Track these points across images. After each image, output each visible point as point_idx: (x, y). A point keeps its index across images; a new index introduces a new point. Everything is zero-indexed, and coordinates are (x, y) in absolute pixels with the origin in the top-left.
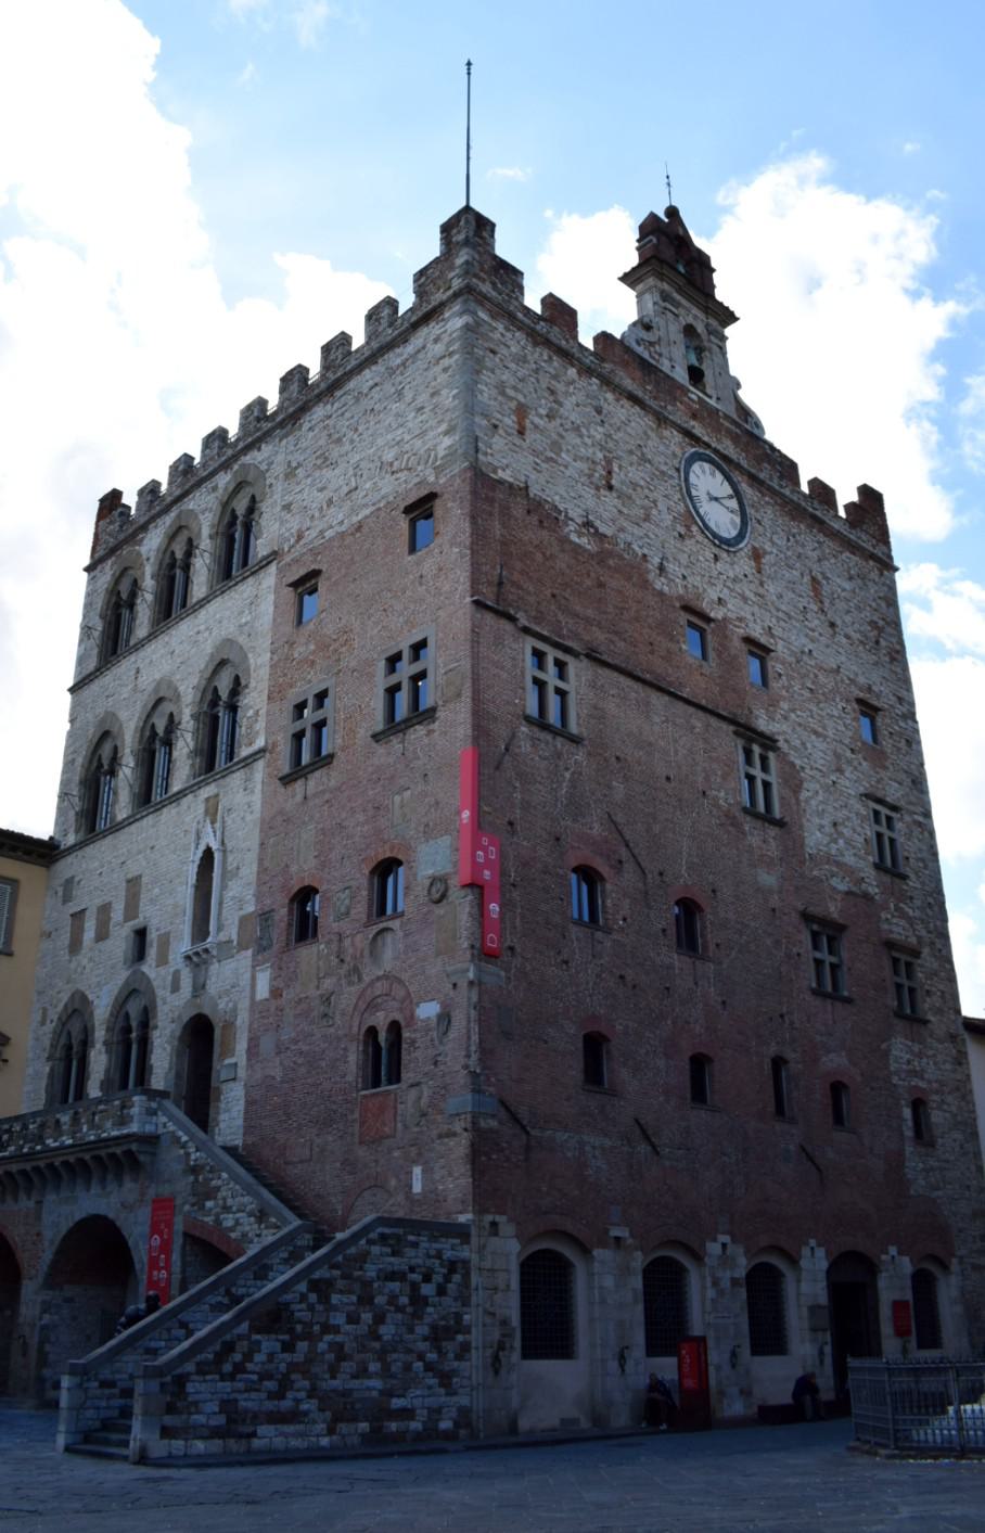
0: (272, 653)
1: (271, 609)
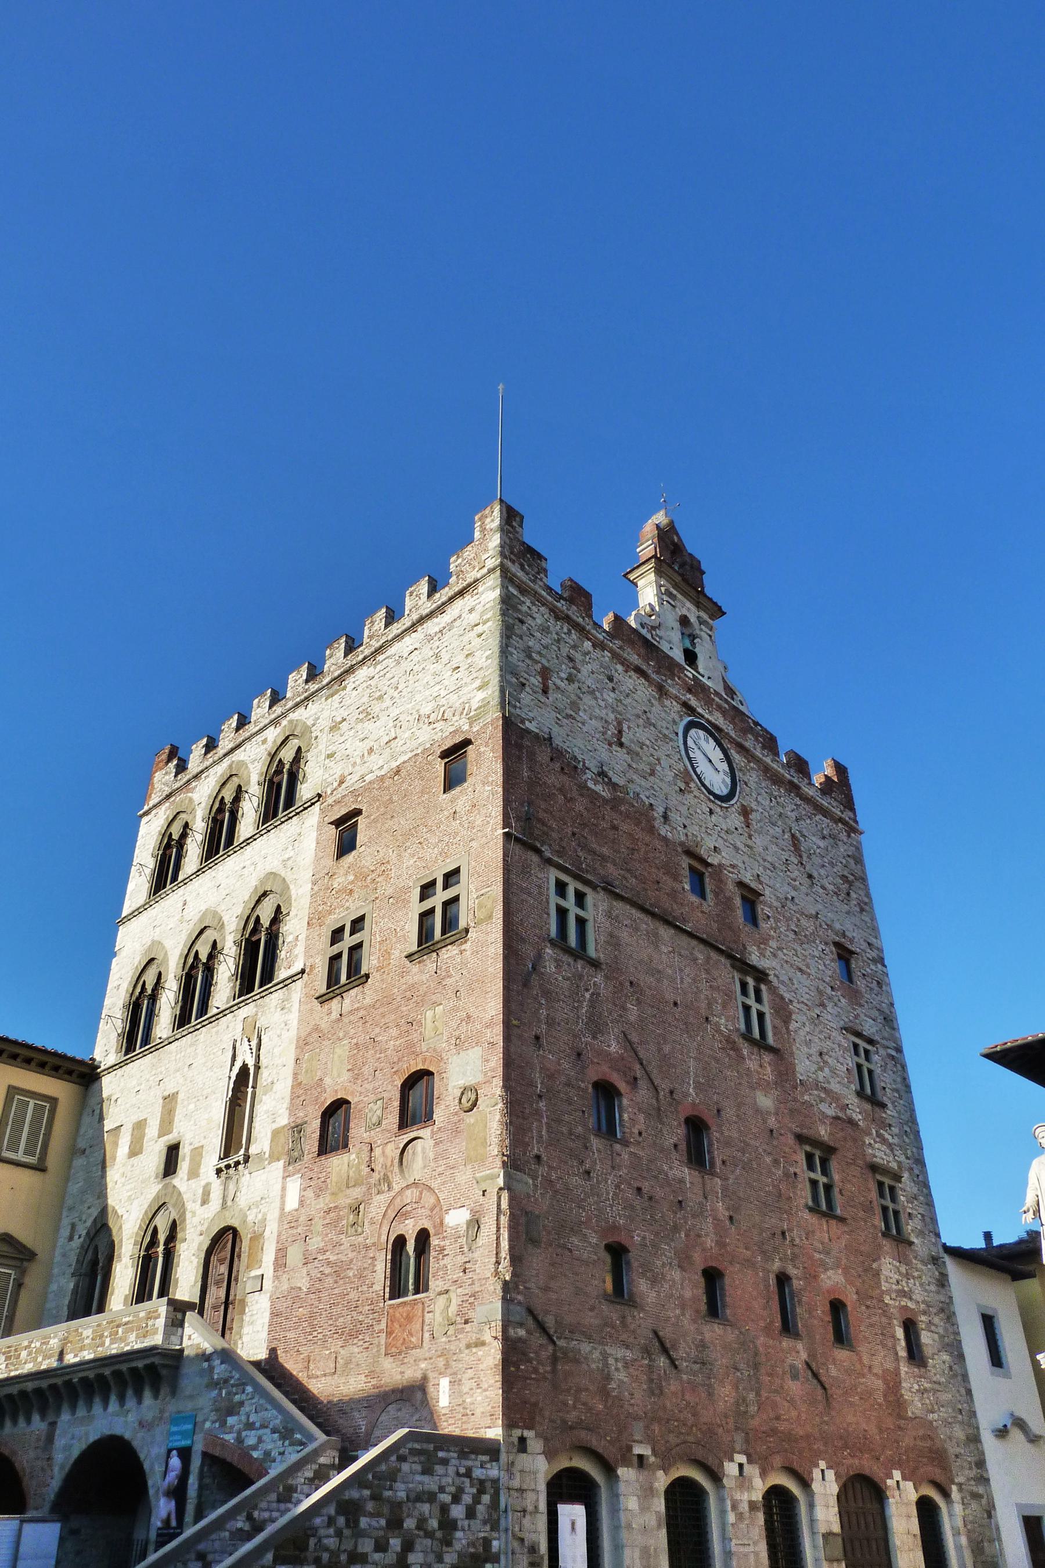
0: (314, 883)
1: (314, 845)
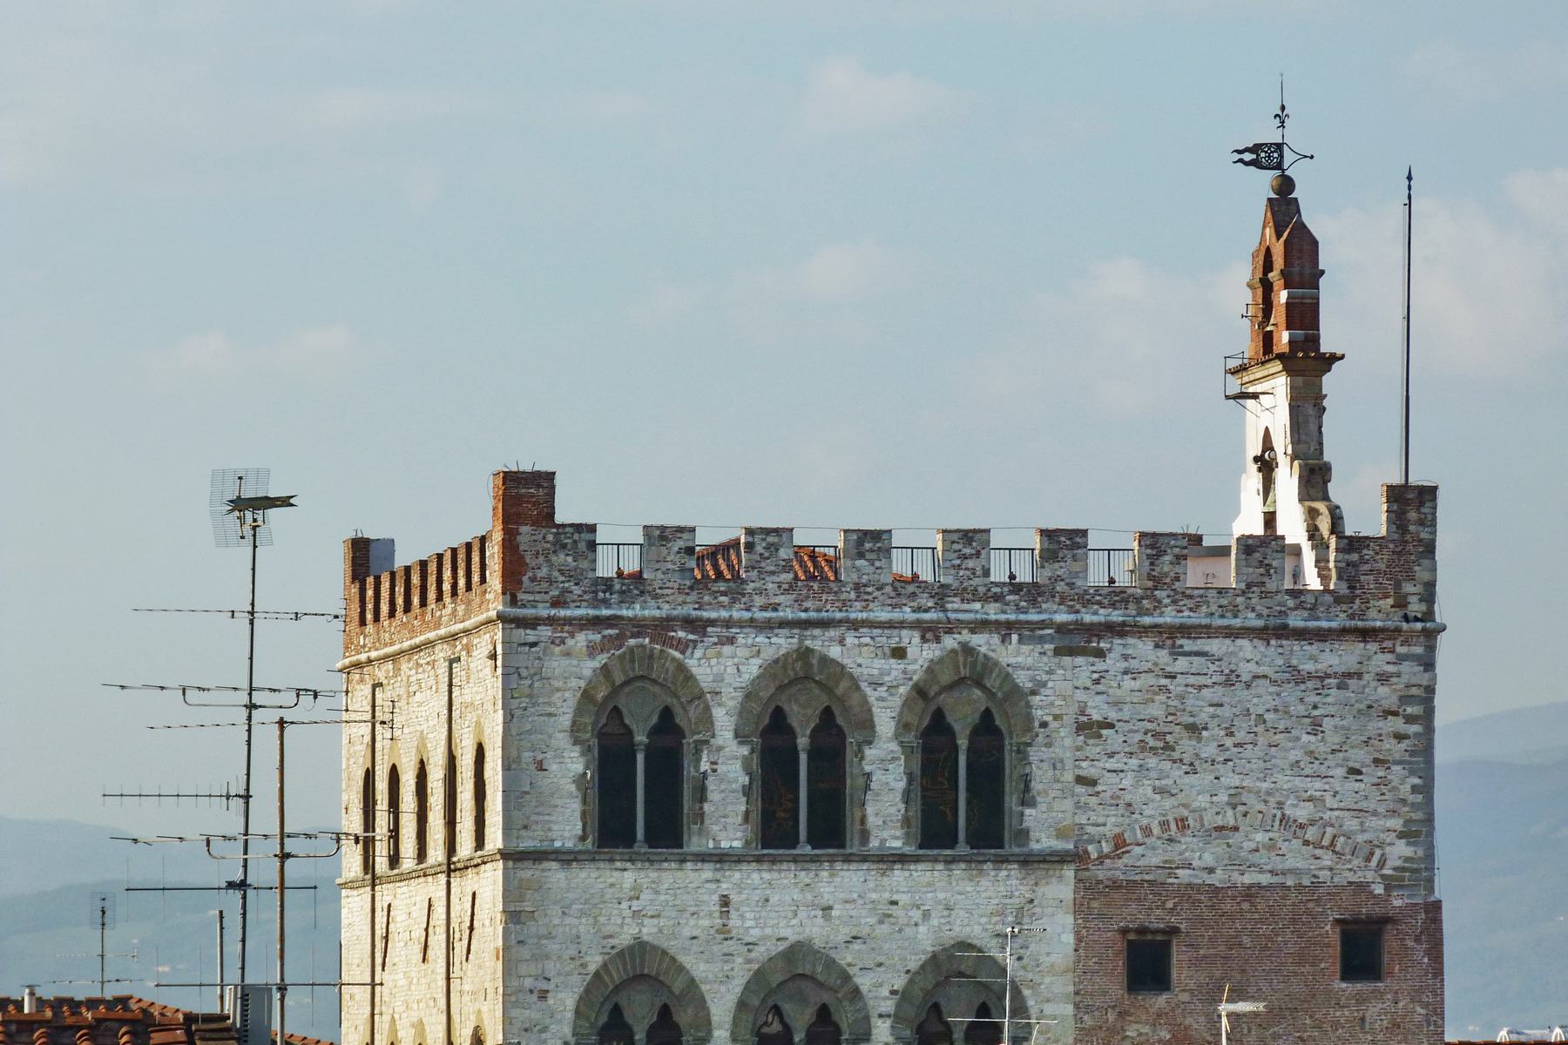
1: (1069, 939)
